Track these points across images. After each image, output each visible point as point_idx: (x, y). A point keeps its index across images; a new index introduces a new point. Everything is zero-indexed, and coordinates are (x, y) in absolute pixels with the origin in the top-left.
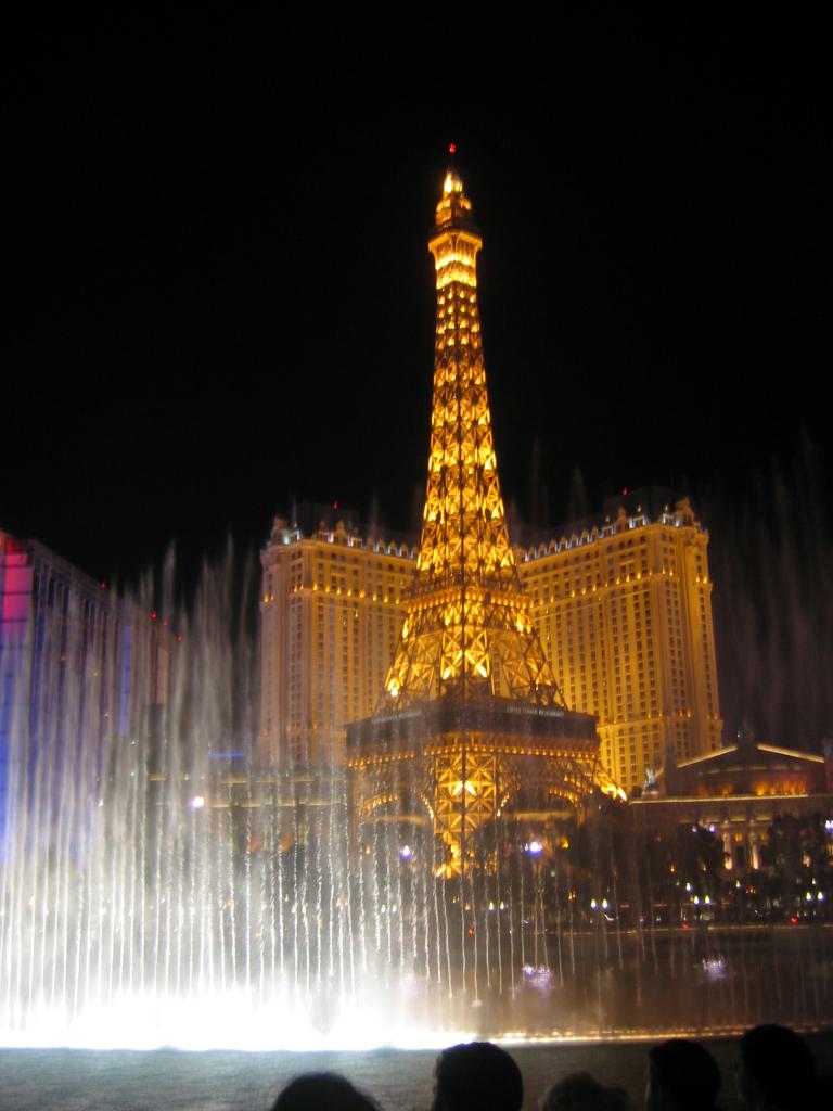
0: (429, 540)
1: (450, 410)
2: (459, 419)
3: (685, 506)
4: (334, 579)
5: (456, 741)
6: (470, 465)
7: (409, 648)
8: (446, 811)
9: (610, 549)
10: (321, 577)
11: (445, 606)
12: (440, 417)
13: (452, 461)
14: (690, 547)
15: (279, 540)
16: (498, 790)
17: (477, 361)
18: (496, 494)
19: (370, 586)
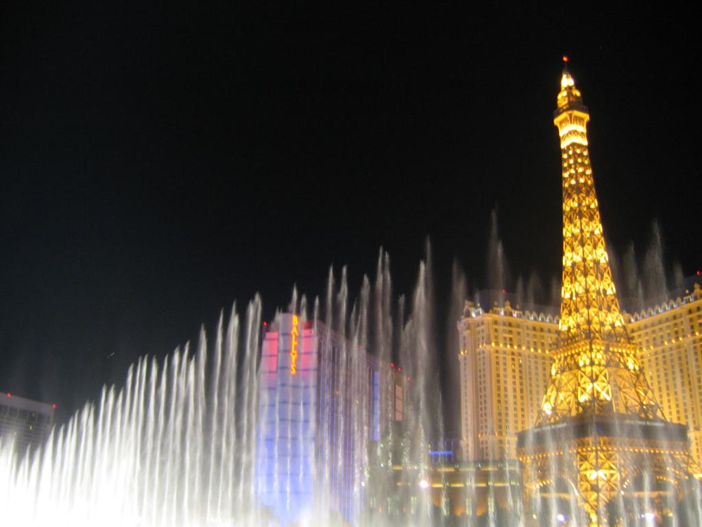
0: (566, 311)
1: (575, 225)
2: (582, 231)
4: (505, 338)
5: (590, 443)
6: (591, 261)
7: (556, 383)
8: (586, 490)
9: (690, 312)
10: (496, 337)
11: (579, 354)
12: (569, 230)
13: (578, 259)
15: (468, 315)
16: (621, 476)
17: (591, 193)
18: (609, 278)
19: (528, 342)
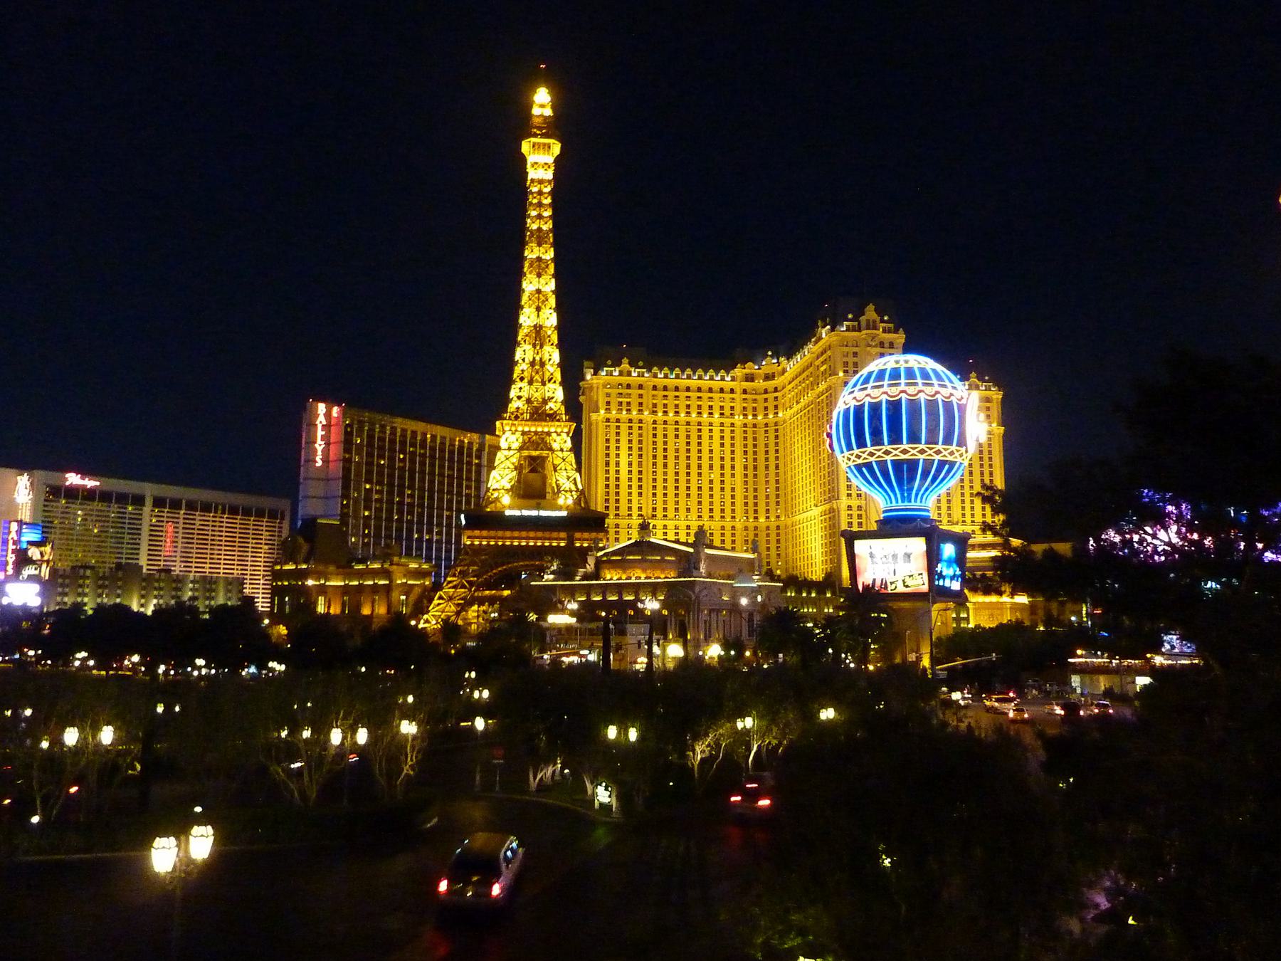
3: (870, 313)
4: (621, 403)
10: (608, 403)
19: (655, 405)
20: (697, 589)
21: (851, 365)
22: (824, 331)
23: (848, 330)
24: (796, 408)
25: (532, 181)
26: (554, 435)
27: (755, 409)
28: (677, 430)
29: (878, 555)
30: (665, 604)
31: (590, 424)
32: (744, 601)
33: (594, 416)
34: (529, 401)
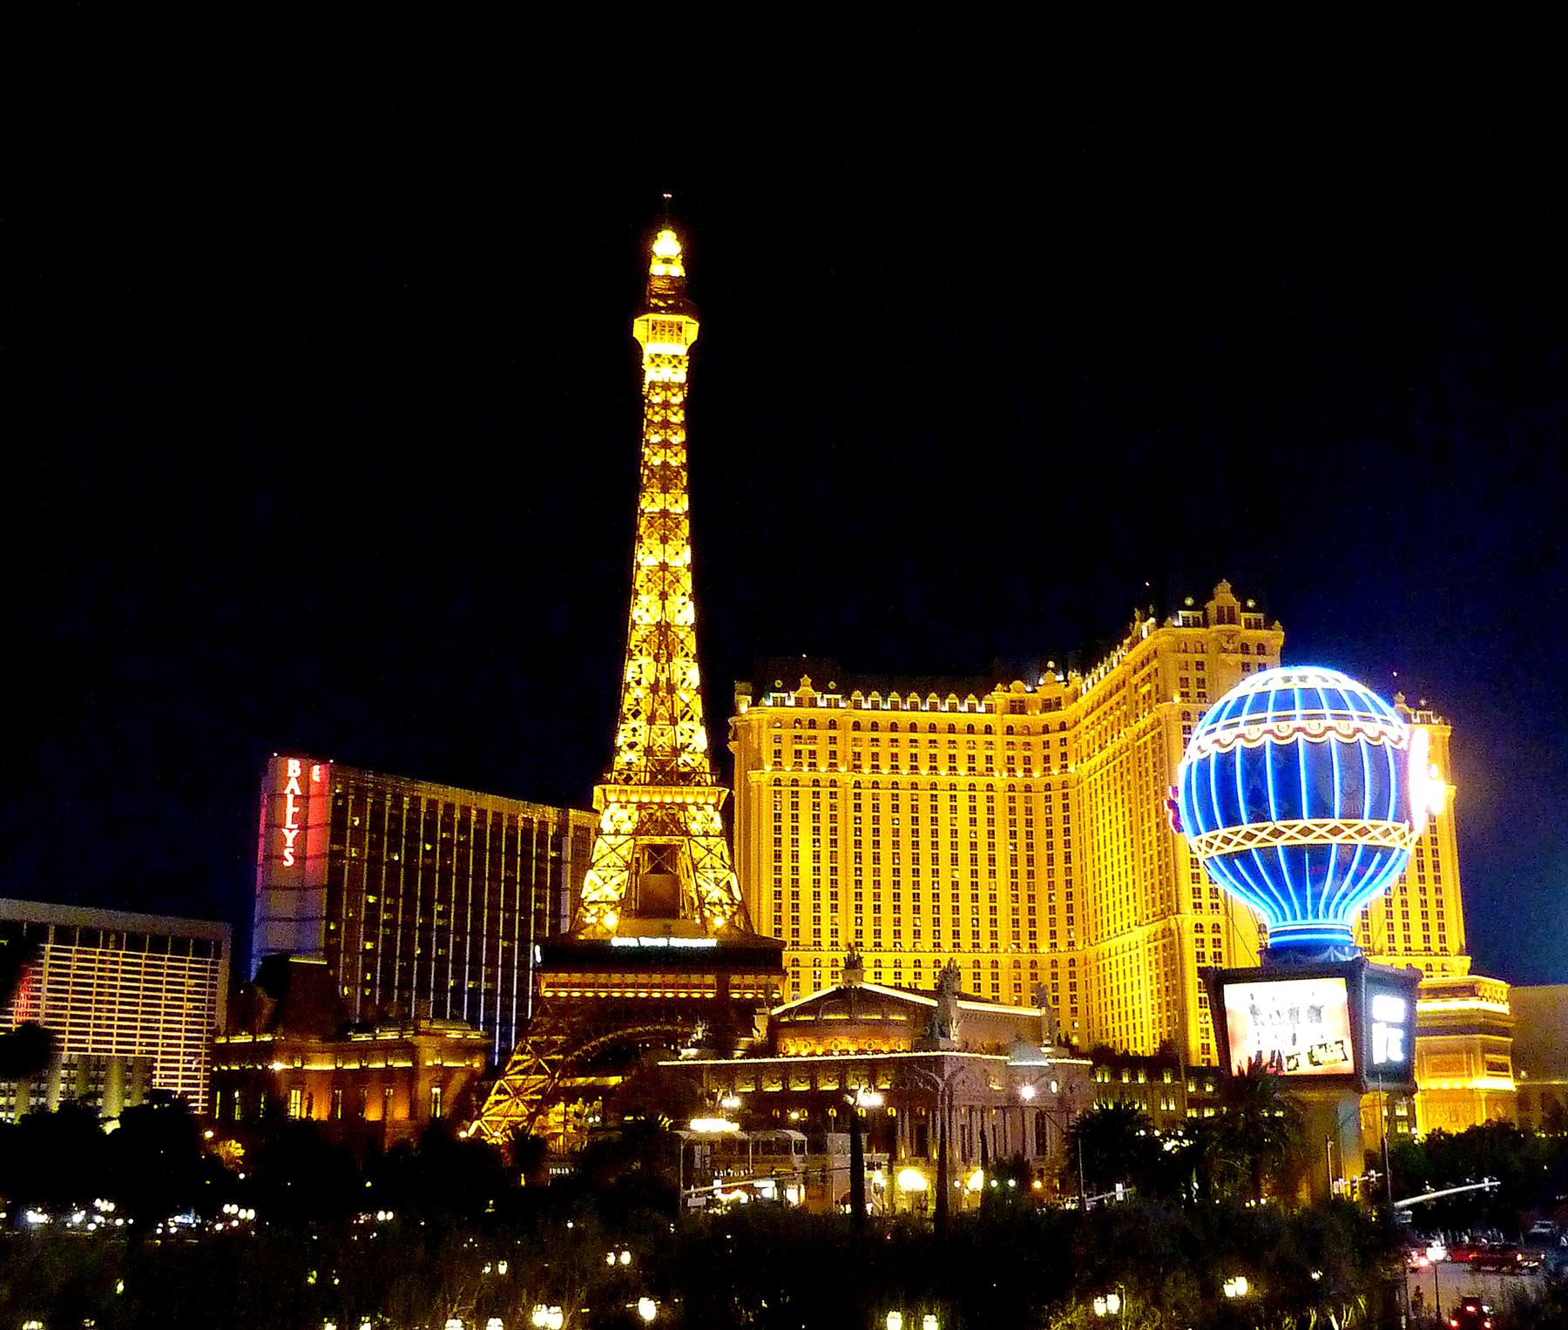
3: (1224, 595)
4: (798, 753)
10: (778, 753)
14: (1223, 656)
19: (857, 756)
20: (947, 1071)
21: (1193, 683)
22: (1144, 627)
23: (1186, 625)
24: (1098, 758)
25: (653, 385)
26: (692, 809)
27: (1027, 760)
28: (895, 797)
29: (1265, 1008)
30: (892, 1097)
31: (748, 789)
32: (1028, 1093)
33: (754, 776)
34: (648, 751)
